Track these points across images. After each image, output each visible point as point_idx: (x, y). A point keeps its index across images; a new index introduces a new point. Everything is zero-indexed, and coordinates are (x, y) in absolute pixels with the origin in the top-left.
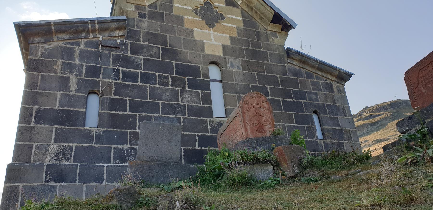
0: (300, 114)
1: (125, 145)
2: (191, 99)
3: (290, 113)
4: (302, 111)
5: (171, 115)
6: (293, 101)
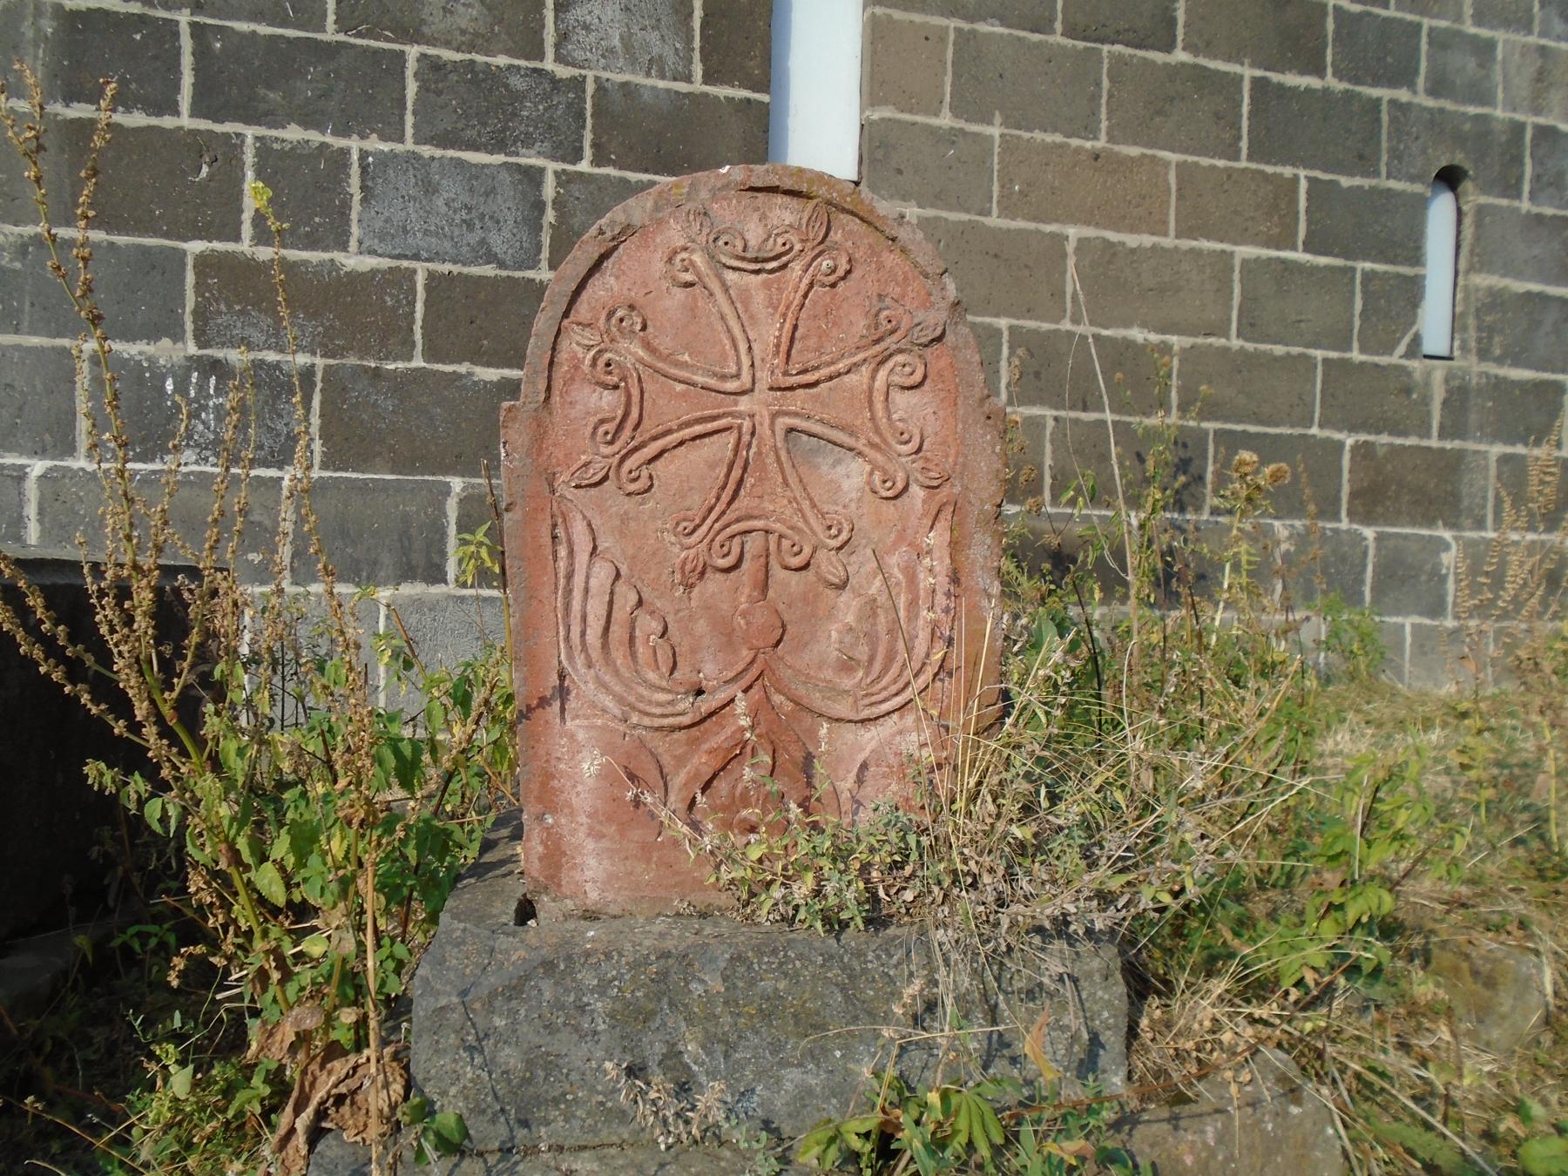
0: (1345, 182)
1: (166, 342)
2: (626, 41)
3: (1288, 171)
4: (1364, 162)
5: (475, 147)
6: (1326, 91)
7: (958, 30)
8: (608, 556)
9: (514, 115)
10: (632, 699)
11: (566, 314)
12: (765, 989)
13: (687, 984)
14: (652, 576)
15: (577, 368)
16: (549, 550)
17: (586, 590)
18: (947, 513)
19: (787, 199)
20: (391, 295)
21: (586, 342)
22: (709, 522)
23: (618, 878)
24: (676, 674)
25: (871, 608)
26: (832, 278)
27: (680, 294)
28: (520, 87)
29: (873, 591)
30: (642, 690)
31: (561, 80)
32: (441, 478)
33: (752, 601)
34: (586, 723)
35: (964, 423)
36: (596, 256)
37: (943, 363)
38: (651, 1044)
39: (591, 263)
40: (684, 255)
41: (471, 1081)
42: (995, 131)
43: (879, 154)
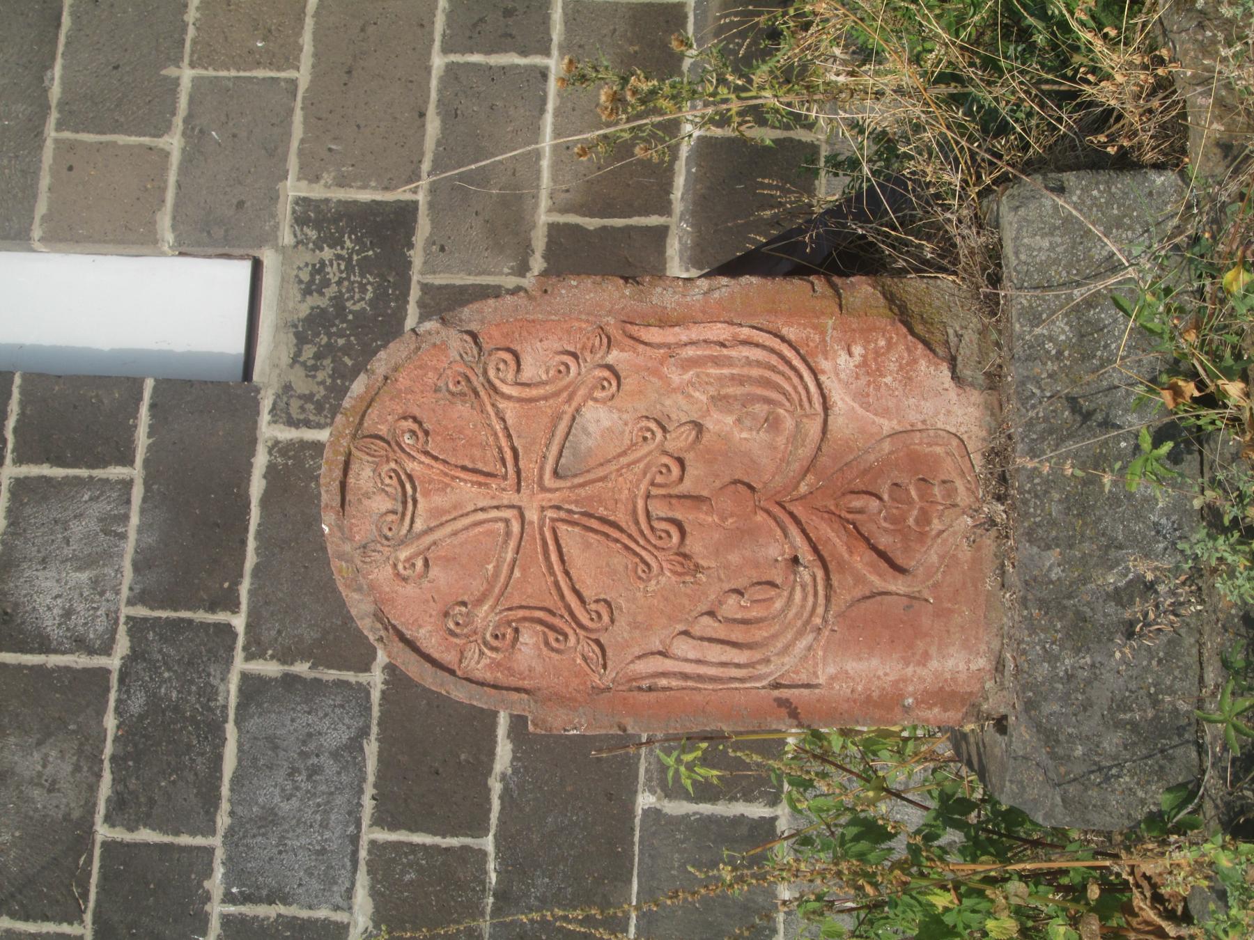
2: (84, 563)
5: (219, 758)
7: (60, 126)
8: (668, 641)
9: (176, 709)
10: (799, 623)
11: (452, 672)
12: (1060, 512)
13: (1051, 582)
14: (687, 602)
15: (499, 665)
16: (661, 695)
17: (698, 662)
18: (633, 330)
19: (351, 474)
20: (403, 873)
21: (476, 656)
22: (638, 549)
23: (967, 640)
24: (778, 582)
25: (721, 401)
26: (421, 434)
27: (434, 571)
28: (142, 701)
29: (704, 398)
30: (791, 614)
31: (132, 648)
32: (637, 821)
33: (711, 511)
34: (820, 665)
35: (550, 313)
36: (401, 645)
37: (496, 333)
38: (1106, 615)
39: (407, 650)
40: (400, 567)
41: (1132, 777)
42: (187, 75)
43: (219, 232)
